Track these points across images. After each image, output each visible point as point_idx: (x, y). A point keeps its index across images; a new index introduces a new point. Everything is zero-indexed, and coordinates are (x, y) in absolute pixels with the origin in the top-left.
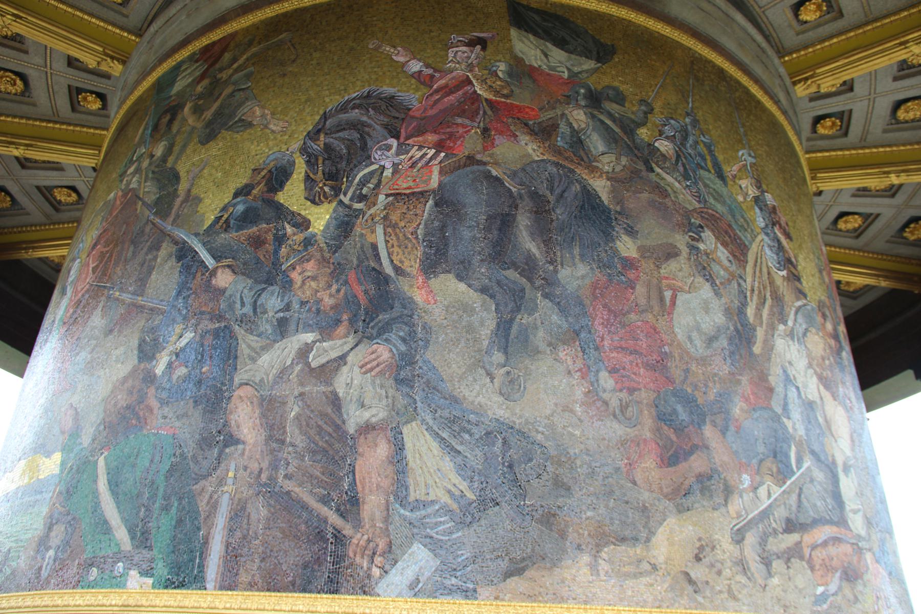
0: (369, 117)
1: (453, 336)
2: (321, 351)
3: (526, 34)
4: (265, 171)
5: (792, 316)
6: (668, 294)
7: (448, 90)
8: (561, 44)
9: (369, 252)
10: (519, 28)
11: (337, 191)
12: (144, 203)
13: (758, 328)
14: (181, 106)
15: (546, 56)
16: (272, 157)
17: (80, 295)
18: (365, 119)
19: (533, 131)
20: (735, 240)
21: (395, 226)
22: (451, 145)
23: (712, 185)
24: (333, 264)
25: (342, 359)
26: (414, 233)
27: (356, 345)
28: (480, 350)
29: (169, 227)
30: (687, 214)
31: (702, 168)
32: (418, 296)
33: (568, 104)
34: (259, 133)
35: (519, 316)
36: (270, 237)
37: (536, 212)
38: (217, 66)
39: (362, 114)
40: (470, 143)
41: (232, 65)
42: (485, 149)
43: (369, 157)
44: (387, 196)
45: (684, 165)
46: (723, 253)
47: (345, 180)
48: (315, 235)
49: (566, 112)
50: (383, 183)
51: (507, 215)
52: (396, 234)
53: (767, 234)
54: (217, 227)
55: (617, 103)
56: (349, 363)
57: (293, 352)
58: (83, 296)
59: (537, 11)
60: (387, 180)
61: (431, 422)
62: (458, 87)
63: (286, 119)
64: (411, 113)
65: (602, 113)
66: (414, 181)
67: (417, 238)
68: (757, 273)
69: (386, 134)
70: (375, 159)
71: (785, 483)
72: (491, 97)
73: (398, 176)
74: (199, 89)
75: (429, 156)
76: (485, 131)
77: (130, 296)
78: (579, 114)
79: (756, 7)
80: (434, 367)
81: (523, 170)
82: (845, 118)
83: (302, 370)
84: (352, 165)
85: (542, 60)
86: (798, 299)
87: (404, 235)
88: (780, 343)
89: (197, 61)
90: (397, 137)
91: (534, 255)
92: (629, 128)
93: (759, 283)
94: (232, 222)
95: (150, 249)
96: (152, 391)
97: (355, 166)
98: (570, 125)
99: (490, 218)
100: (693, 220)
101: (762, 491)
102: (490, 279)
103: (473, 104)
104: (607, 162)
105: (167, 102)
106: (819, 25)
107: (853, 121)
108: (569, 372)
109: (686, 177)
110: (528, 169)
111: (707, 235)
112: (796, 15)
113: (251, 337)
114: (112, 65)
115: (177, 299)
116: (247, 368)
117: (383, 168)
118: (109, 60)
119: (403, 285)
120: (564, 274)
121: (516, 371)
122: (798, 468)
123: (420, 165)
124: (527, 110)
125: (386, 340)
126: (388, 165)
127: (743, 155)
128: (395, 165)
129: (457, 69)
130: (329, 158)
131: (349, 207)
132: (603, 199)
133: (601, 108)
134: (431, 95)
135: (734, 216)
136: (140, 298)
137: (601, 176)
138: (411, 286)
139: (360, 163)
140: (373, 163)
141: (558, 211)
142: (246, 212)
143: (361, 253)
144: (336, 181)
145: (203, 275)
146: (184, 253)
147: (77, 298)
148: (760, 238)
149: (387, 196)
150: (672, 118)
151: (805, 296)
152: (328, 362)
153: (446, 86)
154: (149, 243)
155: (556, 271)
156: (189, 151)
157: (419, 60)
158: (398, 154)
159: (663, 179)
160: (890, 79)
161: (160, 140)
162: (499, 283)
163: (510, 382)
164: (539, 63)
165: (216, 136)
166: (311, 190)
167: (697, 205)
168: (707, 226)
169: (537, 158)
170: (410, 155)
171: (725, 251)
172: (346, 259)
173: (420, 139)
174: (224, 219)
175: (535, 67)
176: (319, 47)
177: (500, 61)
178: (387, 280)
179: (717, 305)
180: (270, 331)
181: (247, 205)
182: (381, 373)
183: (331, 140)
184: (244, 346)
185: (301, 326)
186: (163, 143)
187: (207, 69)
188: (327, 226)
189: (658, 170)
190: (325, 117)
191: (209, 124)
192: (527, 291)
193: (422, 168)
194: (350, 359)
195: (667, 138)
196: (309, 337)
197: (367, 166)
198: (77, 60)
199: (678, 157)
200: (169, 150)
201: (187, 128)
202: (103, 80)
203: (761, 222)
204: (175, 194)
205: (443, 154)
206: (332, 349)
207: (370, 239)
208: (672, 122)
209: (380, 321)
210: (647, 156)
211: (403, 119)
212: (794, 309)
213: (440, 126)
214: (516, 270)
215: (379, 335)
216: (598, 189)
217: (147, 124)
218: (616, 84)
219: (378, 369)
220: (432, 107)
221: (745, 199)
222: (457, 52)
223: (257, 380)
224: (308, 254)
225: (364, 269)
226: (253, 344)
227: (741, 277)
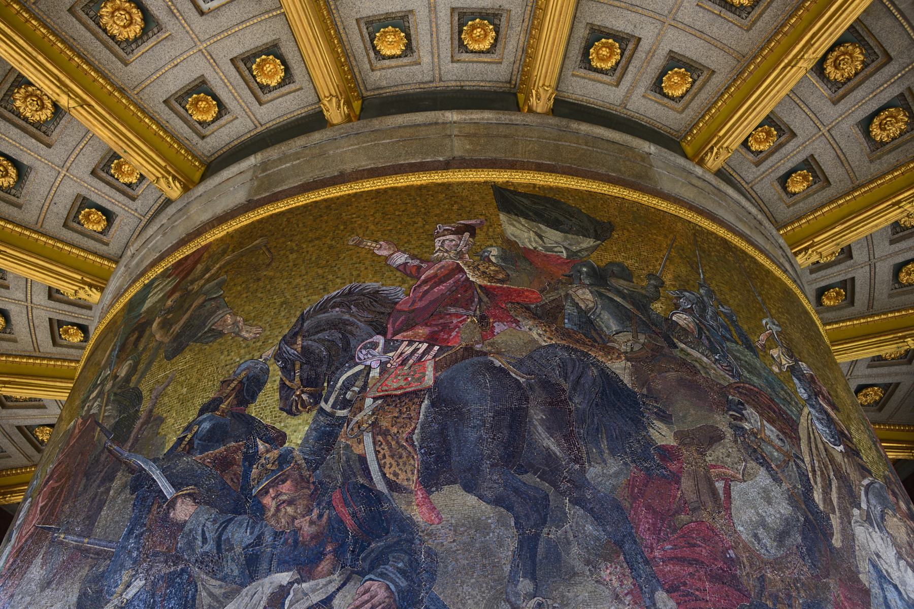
0: (352, 315)
1: (466, 562)
2: (300, 595)
3: (516, 218)
4: (236, 382)
6: (720, 485)
7: (437, 280)
8: (555, 225)
10: (508, 212)
11: (317, 398)
12: (103, 429)
14: (150, 323)
15: (541, 237)
16: (243, 367)
18: (346, 317)
19: (536, 314)
20: (782, 415)
21: (386, 433)
22: (446, 336)
23: (742, 358)
24: (314, 483)
26: (409, 440)
27: (344, 584)
30: (723, 391)
31: (728, 340)
32: (418, 514)
35: (546, 530)
36: (239, 457)
37: (550, 404)
38: (189, 278)
39: (344, 312)
40: (465, 331)
41: (205, 275)
42: (483, 339)
43: (353, 358)
44: (375, 399)
46: (772, 431)
47: (326, 384)
48: (291, 451)
49: (570, 292)
50: (370, 386)
51: (517, 409)
52: (388, 443)
53: (812, 406)
54: (180, 449)
55: (625, 279)
57: (265, 599)
59: (525, 195)
60: (374, 381)
65: (609, 290)
66: (406, 379)
67: (413, 445)
68: (814, 450)
70: (360, 359)
72: (485, 283)
73: (387, 376)
74: (169, 303)
75: (421, 351)
76: (483, 319)
78: (584, 293)
79: (744, 184)
81: (530, 357)
82: (848, 285)
84: (333, 368)
85: (536, 242)
89: (169, 276)
90: (384, 334)
91: (555, 454)
92: (642, 303)
93: (819, 461)
94: (196, 442)
95: (103, 482)
97: (337, 369)
100: (730, 397)
103: (466, 291)
104: (624, 341)
106: (808, 196)
107: (857, 289)
108: (617, 597)
109: (714, 351)
110: (536, 356)
111: (749, 411)
112: (785, 188)
113: (214, 582)
114: (90, 293)
115: (128, 539)
117: (369, 368)
118: (87, 288)
119: (399, 502)
120: (593, 472)
121: (550, 602)
123: (411, 362)
125: (382, 575)
127: (767, 324)
128: (383, 366)
129: (445, 258)
130: (308, 363)
131: (332, 415)
132: (625, 382)
133: (608, 285)
135: (773, 389)
137: (619, 357)
138: (409, 503)
139: (343, 365)
140: (357, 364)
143: (346, 468)
146: (141, 483)
148: (806, 410)
150: (686, 291)
153: (435, 275)
154: (102, 474)
155: (583, 471)
156: (154, 367)
157: (404, 252)
158: (385, 351)
159: (688, 354)
160: (887, 244)
161: (126, 360)
162: (516, 491)
164: (534, 245)
165: (183, 349)
166: (287, 399)
167: (732, 380)
168: (748, 403)
169: (544, 344)
170: (399, 351)
171: (774, 429)
172: (329, 476)
173: (410, 333)
174: (187, 439)
177: (492, 246)
178: (379, 498)
180: (236, 573)
181: (213, 422)
183: (310, 342)
184: (204, 594)
185: (274, 563)
187: (179, 283)
188: (306, 440)
189: (683, 346)
190: (302, 318)
192: (551, 498)
193: (414, 364)
195: (685, 311)
196: (284, 578)
197: (350, 368)
198: (58, 291)
199: (700, 329)
200: (133, 370)
201: (153, 345)
202: (84, 311)
203: (803, 394)
204: (136, 417)
205: (436, 348)
206: (314, 591)
207: (357, 450)
208: (687, 294)
209: (373, 551)
210: (666, 331)
211: (390, 314)
213: (431, 318)
215: (372, 569)
216: (617, 372)
217: (115, 345)
218: (620, 259)
220: (421, 299)
221: (780, 369)
227: (798, 457)
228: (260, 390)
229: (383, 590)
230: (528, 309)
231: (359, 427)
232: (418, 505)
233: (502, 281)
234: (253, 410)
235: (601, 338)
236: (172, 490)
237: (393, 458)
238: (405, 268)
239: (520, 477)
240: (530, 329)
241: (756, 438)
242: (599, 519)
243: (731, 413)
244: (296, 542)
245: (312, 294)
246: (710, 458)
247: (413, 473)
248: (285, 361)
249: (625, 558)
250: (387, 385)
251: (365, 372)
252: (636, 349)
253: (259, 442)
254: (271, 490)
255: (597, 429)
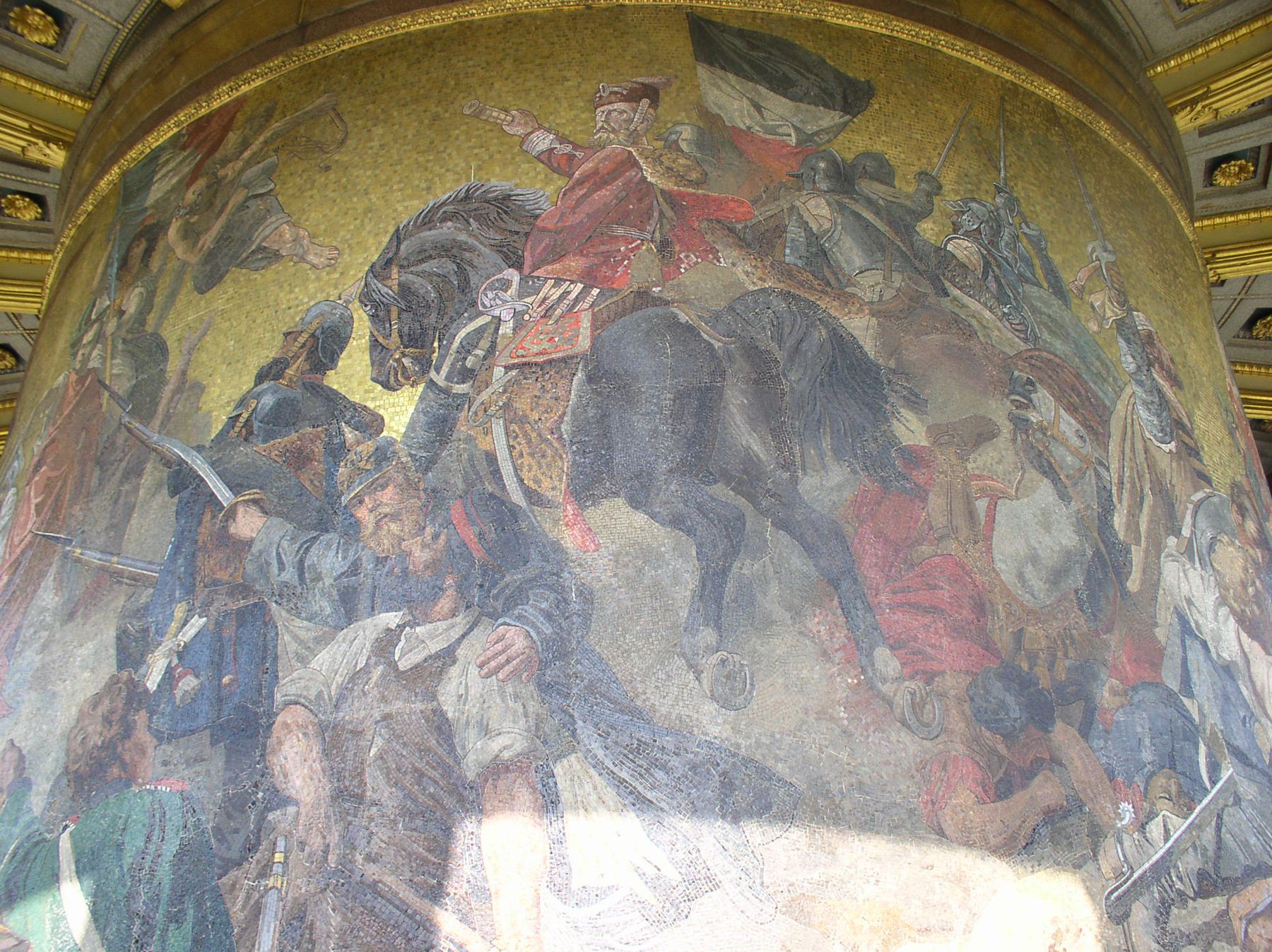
1: (630, 604)
4: (305, 335)
5: (1188, 519)
6: (981, 505)
7: (598, 180)
8: (782, 86)
9: (483, 467)
10: (711, 64)
11: (425, 365)
12: (113, 395)
13: (1133, 548)
14: (162, 227)
15: (758, 108)
16: (313, 313)
17: (18, 551)
18: (463, 237)
19: (743, 240)
20: (1088, 399)
21: (523, 420)
22: (609, 273)
23: (1045, 309)
24: (425, 490)
25: (448, 656)
27: (471, 629)
28: (675, 626)
29: (156, 437)
30: (1007, 364)
31: (1027, 281)
32: (569, 539)
33: (799, 189)
34: (292, 270)
35: (737, 564)
36: (319, 448)
38: (217, 155)
39: (460, 230)
41: (241, 153)
42: (665, 278)
43: (473, 304)
44: (508, 368)
45: (996, 279)
46: (1070, 424)
47: (436, 344)
48: (392, 442)
49: (797, 203)
50: (499, 348)
51: (709, 389)
52: (526, 435)
53: (1140, 383)
54: (233, 434)
55: (881, 182)
56: (461, 660)
57: (368, 645)
58: (23, 552)
59: (741, 33)
60: (506, 342)
61: (600, 753)
62: (614, 174)
63: (335, 244)
64: (539, 222)
65: (857, 201)
66: (551, 339)
67: (560, 438)
68: (1127, 450)
69: (500, 261)
70: (484, 305)
71: (1191, 810)
72: (670, 186)
73: (523, 333)
74: (190, 196)
75: (573, 296)
76: (664, 246)
77: (99, 556)
78: (817, 206)
80: (601, 659)
81: (731, 309)
83: (383, 676)
84: (446, 320)
85: (751, 117)
86: (1196, 490)
87: (539, 435)
88: (1171, 571)
89: (184, 148)
90: (518, 266)
91: (757, 456)
92: (903, 221)
93: (1132, 469)
94: (256, 424)
95: (126, 476)
96: (141, 718)
97: (452, 320)
98: (805, 225)
99: (679, 396)
100: (1016, 373)
101: (1155, 829)
102: (685, 502)
103: (640, 200)
104: (869, 285)
105: (140, 218)
109: (1002, 298)
110: (740, 308)
111: (1043, 396)
113: (298, 622)
115: (176, 560)
116: (295, 675)
117: (498, 320)
120: (808, 484)
121: (737, 658)
122: (1214, 783)
123: (558, 312)
124: (732, 205)
125: (519, 618)
126: (506, 315)
127: (1094, 250)
128: (517, 314)
129: (611, 143)
130: (409, 309)
131: (446, 391)
132: (867, 349)
134: (572, 189)
135: (1083, 359)
136: (115, 559)
137: (860, 310)
138: (556, 522)
140: (481, 314)
141: (793, 377)
142: (278, 405)
144: (423, 347)
145: (214, 517)
146: (181, 481)
147: (14, 557)
148: (1128, 390)
149: (508, 368)
150: (974, 200)
151: (1209, 481)
152: (425, 660)
153: (595, 172)
154: (124, 464)
155: (794, 481)
157: (549, 130)
158: (521, 296)
159: (964, 306)
161: (132, 285)
162: (700, 508)
163: (727, 677)
164: (748, 122)
165: (222, 277)
166: (382, 365)
168: (1041, 381)
169: (752, 288)
170: (541, 295)
171: (1073, 421)
172: (447, 482)
173: (557, 266)
174: (242, 420)
175: (741, 130)
176: (382, 117)
178: (514, 512)
179: (1063, 516)
180: (328, 610)
182: (515, 674)
184: (287, 638)
185: (378, 601)
186: (137, 291)
187: (201, 162)
188: (411, 426)
189: (957, 292)
190: (398, 237)
191: (210, 256)
193: (562, 316)
194: (460, 652)
195: (967, 234)
196: (391, 619)
197: (471, 319)
199: (987, 265)
200: (147, 304)
201: (173, 265)
203: (1129, 364)
204: (161, 380)
205: (595, 292)
206: (432, 636)
207: (484, 444)
208: (974, 205)
209: (507, 586)
210: (936, 269)
211: (527, 235)
212: (1191, 506)
213: (589, 243)
214: (728, 484)
215: (507, 610)
216: (856, 333)
217: (110, 257)
218: (878, 148)
219: (508, 669)
220: (573, 210)
221: (1100, 326)
222: (610, 112)
223: (313, 694)
224: (382, 476)
225: (476, 498)
226: (302, 634)
227: (1101, 463)
228: (342, 349)
229: (521, 639)
230: (731, 230)
231: (485, 411)
232: (567, 525)
233: (697, 184)
234: (333, 380)
235: (838, 279)
236: (228, 494)
237: (533, 458)
238: (549, 159)
239: (708, 488)
240: (734, 264)
241: (1045, 434)
242: (809, 549)
243: (1013, 397)
244: (405, 571)
245: (411, 198)
246: (974, 465)
247: (561, 480)
248: (376, 305)
249: (840, 603)
250: (523, 348)
251: (493, 326)
252: (886, 297)
253: (347, 429)
254: (367, 499)
255: (819, 421)
